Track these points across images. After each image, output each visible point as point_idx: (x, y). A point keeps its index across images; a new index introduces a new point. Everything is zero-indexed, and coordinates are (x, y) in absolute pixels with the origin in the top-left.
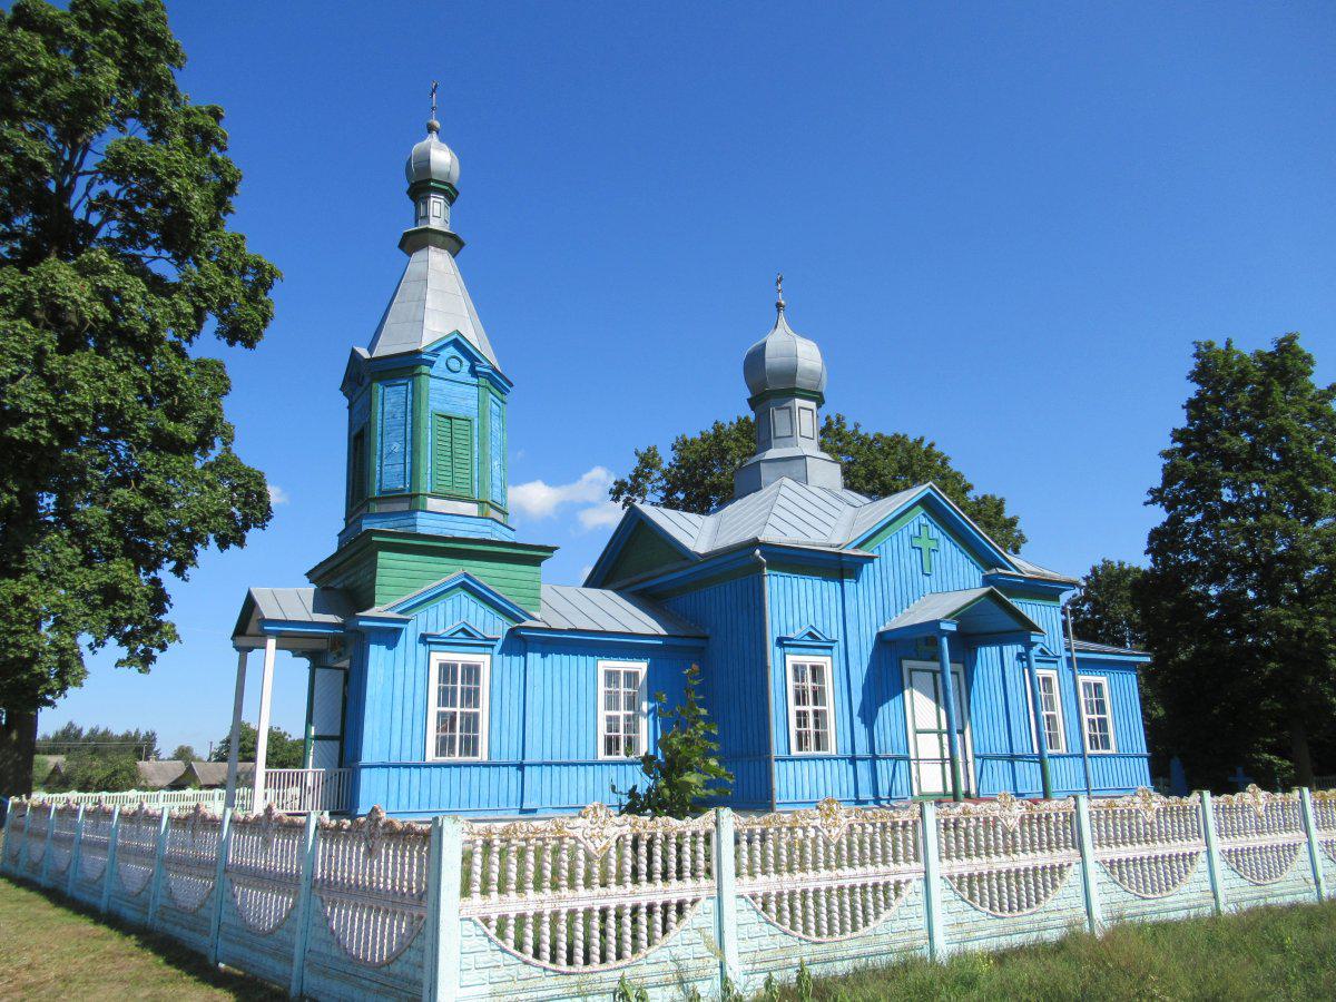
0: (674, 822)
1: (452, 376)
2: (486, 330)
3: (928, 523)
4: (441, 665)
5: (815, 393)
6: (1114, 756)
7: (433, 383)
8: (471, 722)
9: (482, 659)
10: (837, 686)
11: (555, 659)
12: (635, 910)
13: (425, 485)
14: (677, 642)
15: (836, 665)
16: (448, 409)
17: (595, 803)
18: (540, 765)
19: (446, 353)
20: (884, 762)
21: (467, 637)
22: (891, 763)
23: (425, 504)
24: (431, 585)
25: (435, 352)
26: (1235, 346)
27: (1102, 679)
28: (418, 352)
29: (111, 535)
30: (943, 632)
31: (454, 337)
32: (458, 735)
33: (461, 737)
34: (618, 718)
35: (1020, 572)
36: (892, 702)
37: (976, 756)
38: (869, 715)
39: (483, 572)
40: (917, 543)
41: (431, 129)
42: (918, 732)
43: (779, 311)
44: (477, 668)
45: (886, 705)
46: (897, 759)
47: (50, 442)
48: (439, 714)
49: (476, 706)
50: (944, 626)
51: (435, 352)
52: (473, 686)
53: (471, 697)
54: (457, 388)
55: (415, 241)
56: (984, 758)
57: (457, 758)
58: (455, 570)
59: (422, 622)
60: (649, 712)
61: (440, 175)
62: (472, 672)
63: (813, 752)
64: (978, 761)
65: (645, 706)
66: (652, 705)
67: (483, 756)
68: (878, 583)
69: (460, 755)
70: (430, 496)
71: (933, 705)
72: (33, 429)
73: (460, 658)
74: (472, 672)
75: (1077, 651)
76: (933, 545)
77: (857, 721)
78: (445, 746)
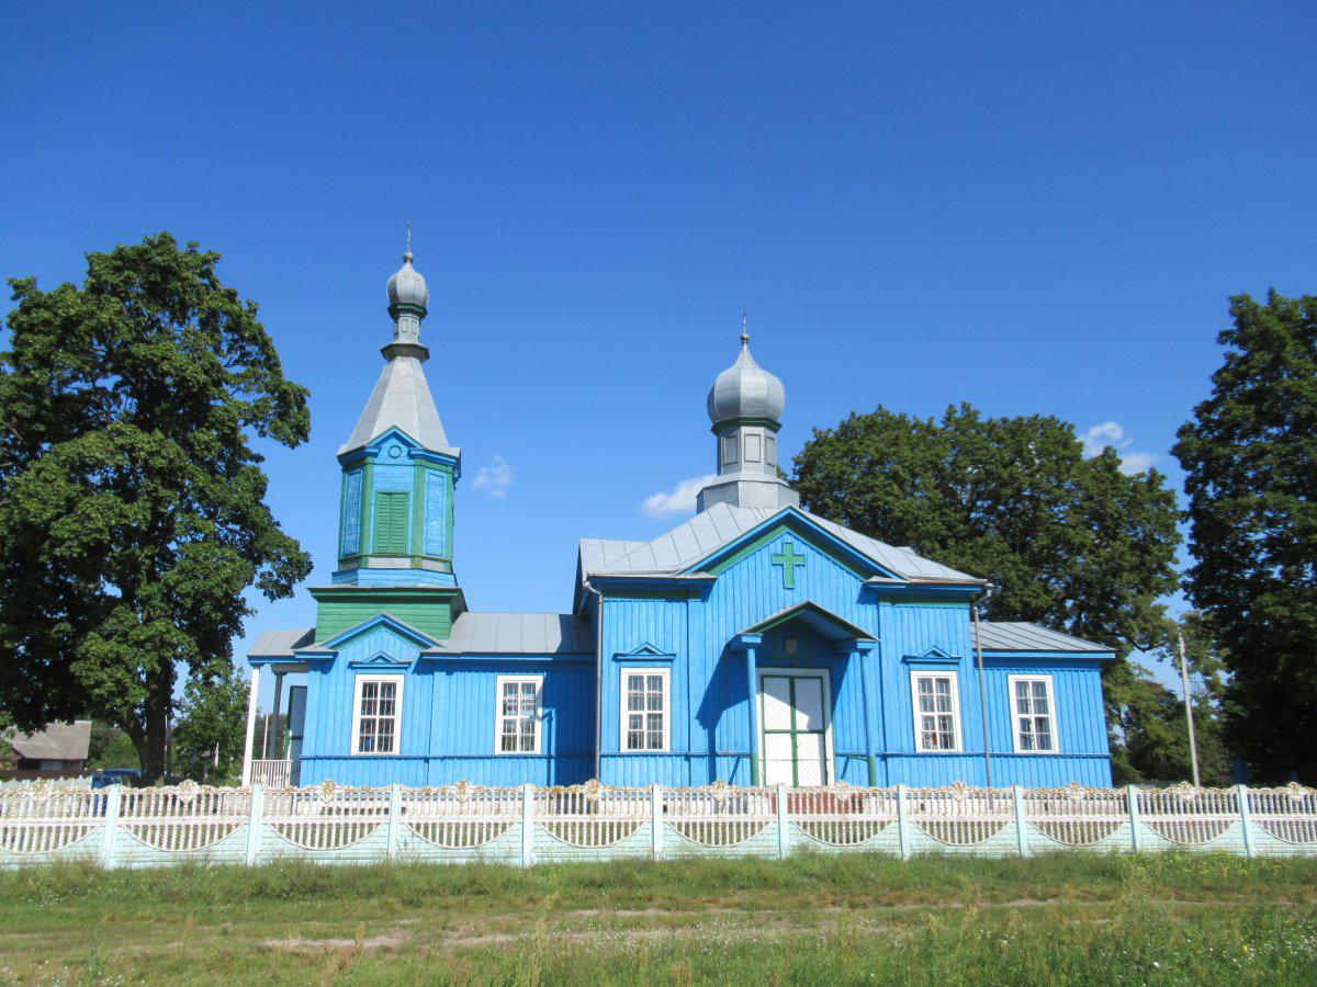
0: (213, 788)
1: (393, 461)
2: (441, 418)
3: (794, 540)
4: (365, 685)
5: (763, 419)
6: (1056, 756)
7: (376, 468)
8: (387, 726)
9: (398, 679)
10: (677, 692)
11: (459, 676)
12: (58, 829)
13: (369, 548)
14: (567, 658)
15: (676, 677)
16: (388, 487)
17: (416, 789)
18: (443, 758)
19: (387, 445)
20: (724, 760)
21: (382, 662)
22: (732, 761)
23: (367, 562)
24: (357, 624)
25: (378, 446)
26: (1281, 293)
27: (1047, 679)
28: (363, 448)
29: (162, 601)
30: (749, 645)
31: (392, 431)
32: (377, 735)
33: (374, 732)
34: (641, 717)
35: (901, 578)
36: (738, 707)
37: (837, 755)
38: (709, 716)
39: (396, 612)
40: (778, 560)
41: (405, 259)
42: (765, 732)
43: (743, 344)
44: (660, 678)
45: (732, 708)
46: (739, 757)
47: (80, 554)
48: (363, 721)
49: (661, 709)
50: (745, 639)
51: (378, 446)
52: (658, 692)
53: (388, 707)
54: (403, 469)
55: (390, 352)
56: (848, 757)
57: (376, 752)
58: (373, 611)
59: (347, 654)
60: (543, 717)
61: (407, 299)
62: (389, 688)
63: (1036, 750)
64: (842, 760)
65: (540, 712)
66: (547, 711)
67: (396, 751)
68: (730, 600)
69: (649, 747)
70: (371, 556)
71: (787, 708)
72: (69, 548)
73: (379, 678)
74: (389, 688)
75: (984, 650)
76: (798, 561)
77: (695, 724)
78: (366, 743)
